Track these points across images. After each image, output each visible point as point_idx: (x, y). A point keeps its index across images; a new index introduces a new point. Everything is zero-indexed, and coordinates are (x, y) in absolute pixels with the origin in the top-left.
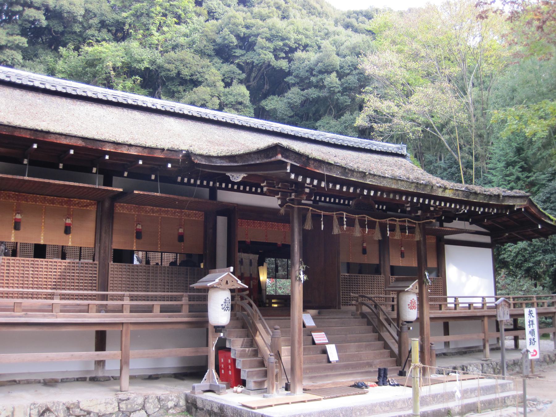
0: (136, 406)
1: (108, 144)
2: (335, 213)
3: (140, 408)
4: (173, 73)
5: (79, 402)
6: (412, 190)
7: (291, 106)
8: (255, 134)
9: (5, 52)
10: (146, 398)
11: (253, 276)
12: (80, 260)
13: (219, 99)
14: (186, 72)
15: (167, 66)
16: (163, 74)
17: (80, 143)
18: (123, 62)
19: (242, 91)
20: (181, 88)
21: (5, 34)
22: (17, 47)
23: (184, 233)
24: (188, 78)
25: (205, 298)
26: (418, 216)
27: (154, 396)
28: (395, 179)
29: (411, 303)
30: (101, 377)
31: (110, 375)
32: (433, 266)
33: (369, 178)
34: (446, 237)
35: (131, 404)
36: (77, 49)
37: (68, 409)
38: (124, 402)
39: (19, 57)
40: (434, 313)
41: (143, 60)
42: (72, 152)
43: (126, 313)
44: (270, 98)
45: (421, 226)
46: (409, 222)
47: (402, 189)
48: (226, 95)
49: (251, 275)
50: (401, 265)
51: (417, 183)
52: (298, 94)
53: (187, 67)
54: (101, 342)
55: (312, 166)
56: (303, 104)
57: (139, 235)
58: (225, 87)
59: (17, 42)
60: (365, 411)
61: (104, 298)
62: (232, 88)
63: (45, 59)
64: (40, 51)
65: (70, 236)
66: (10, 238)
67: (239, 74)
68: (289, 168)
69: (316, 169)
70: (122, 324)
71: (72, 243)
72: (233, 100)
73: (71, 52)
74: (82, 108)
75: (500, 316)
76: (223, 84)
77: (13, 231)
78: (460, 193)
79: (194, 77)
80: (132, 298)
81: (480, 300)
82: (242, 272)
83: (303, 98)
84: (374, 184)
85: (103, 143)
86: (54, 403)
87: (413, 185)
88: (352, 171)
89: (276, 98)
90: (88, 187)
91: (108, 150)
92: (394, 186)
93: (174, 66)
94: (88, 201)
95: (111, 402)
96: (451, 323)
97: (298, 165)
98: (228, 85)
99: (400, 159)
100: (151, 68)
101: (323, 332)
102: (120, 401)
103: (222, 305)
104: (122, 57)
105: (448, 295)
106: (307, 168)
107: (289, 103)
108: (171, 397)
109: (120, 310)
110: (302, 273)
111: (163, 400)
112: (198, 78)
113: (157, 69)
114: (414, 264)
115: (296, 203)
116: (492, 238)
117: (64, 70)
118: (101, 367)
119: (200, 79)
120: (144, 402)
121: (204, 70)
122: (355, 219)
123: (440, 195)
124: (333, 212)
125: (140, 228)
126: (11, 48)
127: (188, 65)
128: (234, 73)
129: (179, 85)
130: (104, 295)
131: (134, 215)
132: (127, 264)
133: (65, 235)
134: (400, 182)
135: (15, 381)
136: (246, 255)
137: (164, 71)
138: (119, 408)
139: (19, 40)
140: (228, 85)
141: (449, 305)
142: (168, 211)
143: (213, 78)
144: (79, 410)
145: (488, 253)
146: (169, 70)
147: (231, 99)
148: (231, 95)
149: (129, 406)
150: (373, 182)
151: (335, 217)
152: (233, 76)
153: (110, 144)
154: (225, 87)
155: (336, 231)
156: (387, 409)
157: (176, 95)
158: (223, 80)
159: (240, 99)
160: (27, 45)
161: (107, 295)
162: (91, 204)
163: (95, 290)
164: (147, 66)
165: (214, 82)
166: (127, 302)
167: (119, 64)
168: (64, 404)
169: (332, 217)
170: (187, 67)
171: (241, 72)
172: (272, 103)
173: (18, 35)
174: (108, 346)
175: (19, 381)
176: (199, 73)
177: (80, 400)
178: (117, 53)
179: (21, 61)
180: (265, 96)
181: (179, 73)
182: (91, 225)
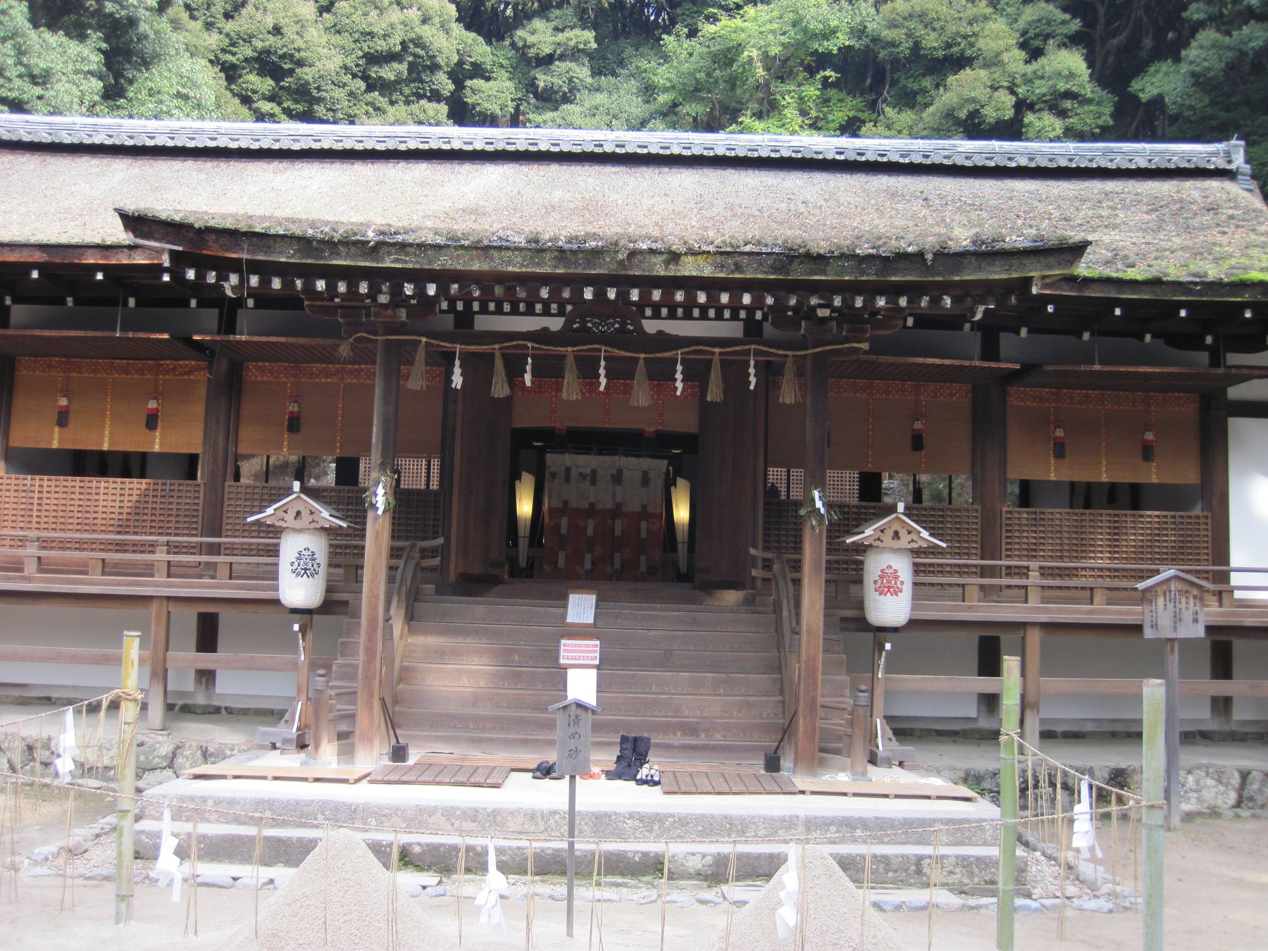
0: (157, 760)
1: (90, 251)
2: (497, 346)
3: (165, 764)
4: (905, 48)
5: (49, 739)
6: (547, 269)
7: (1199, 80)
8: (750, 172)
9: (553, 68)
10: (178, 747)
11: (650, 509)
12: (267, 481)
13: (1013, 93)
14: (931, 41)
15: (888, 34)
16: (882, 54)
17: (39, 257)
18: (783, 44)
19: (1070, 63)
20: (927, 83)
21: (550, 31)
22: (574, 54)
23: (299, 413)
24: (941, 54)
25: (274, 551)
26: (803, 336)
27: (194, 744)
28: (476, 248)
29: (881, 577)
30: (200, 706)
31: (224, 705)
32: (1189, 482)
33: (389, 254)
34: (1236, 392)
35: (145, 753)
36: (693, 33)
37: (30, 748)
39: (582, 72)
40: (1060, 611)
41: (834, 32)
42: (35, 275)
43: (160, 578)
44: (1152, 69)
45: (809, 365)
46: (757, 353)
47: (510, 269)
48: (1031, 81)
49: (644, 507)
50: (1053, 477)
51: (561, 250)
52: (1214, 46)
53: (934, 30)
54: (208, 637)
55: (216, 246)
56: (1232, 67)
57: (294, 424)
58: (1027, 62)
59: (572, 43)
60: (395, 819)
61: (214, 549)
62: (1043, 61)
63: (638, 67)
64: (629, 51)
66: (52, 439)
67: (1063, 22)
69: (227, 250)
70: (151, 598)
71: (161, 446)
72: (1044, 90)
73: (686, 44)
74: (279, 178)
75: (1154, 626)
76: (1021, 55)
77: (57, 429)
78: (745, 260)
79: (955, 49)
80: (173, 548)
82: (619, 499)
83: (1230, 54)
84: (411, 266)
85: (81, 251)
86: (6, 734)
87: (548, 256)
88: (331, 245)
89: (1165, 66)
90: (102, 338)
92: (476, 266)
93: (904, 31)
96: (1240, 647)
98: (1035, 54)
99: (1213, 184)
100: (857, 46)
101: (598, 639)
103: (292, 564)
104: (784, 34)
105: (1235, 561)
106: (205, 252)
107: (1194, 74)
108: (232, 750)
109: (148, 570)
110: (380, 491)
111: (211, 755)
112: (963, 51)
113: (871, 45)
114: (1189, 475)
115: (381, 331)
117: (668, 84)
118: (204, 687)
119: (968, 53)
120: (174, 754)
121: (976, 28)
122: (563, 357)
123: (661, 272)
124: (493, 343)
125: (296, 409)
126: (562, 58)
127: (937, 25)
128: (1049, 23)
129: (924, 75)
130: (211, 545)
131: (286, 383)
132: (119, 480)
134: (496, 254)
135: (49, 699)
136: (632, 460)
137: (883, 48)
139: (576, 36)
140: (1035, 54)
141: (1238, 594)
142: (361, 370)
143: (993, 45)
144: (48, 753)
146: (893, 44)
147: (1041, 88)
148: (1042, 78)
149: (142, 758)
150: (406, 262)
151: (498, 354)
152: (1048, 30)
153: (93, 250)
154: (1027, 62)
155: (500, 389)
156: (467, 825)
157: (919, 99)
158: (1023, 46)
159: (1062, 86)
160: (594, 46)
161: (219, 544)
162: (199, 369)
163: (195, 535)
164: (847, 43)
165: (998, 55)
166: (161, 556)
167: (775, 50)
168: (23, 739)
169: (492, 355)
170: (934, 30)
171: (1067, 17)
172: (1160, 82)
173: (572, 28)
175: (57, 699)
176: (965, 37)
178: (768, 27)
179: (589, 80)
180: (1140, 68)
181: (917, 46)
182: (199, 409)
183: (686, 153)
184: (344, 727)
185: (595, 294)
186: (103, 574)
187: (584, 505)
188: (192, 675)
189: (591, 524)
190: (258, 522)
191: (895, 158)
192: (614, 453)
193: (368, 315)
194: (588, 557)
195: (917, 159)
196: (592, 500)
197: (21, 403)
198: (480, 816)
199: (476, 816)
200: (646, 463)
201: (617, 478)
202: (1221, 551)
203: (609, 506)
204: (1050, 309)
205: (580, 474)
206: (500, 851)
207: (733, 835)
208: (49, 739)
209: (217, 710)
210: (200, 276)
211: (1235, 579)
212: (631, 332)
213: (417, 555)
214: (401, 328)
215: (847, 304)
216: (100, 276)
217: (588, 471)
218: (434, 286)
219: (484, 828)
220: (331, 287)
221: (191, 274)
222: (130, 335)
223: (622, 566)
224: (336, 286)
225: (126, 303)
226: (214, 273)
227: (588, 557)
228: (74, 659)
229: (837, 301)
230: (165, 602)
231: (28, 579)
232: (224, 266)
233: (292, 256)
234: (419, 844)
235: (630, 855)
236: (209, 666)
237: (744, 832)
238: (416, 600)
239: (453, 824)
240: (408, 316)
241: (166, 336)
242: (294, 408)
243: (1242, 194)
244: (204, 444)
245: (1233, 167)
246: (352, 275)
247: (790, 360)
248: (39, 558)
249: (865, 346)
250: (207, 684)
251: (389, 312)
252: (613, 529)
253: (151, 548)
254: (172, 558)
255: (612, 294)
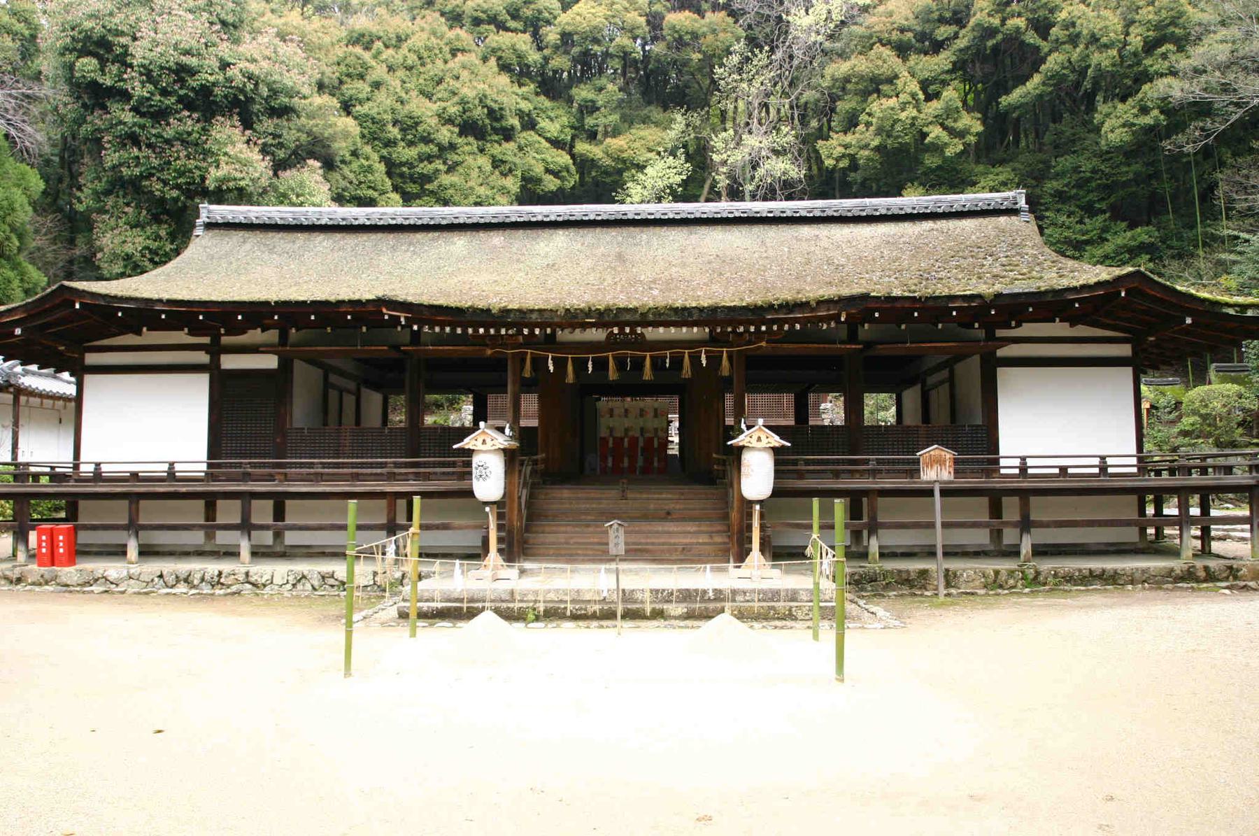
68: (402, 319)
81: (1017, 462)
105: (1002, 453)
116: (1133, 349)
145: (1129, 370)
183: (678, 217)
191: (804, 213)
195: (818, 214)
202: (994, 448)
204: (877, 315)
211: (1003, 462)
215: (747, 331)
243: (1024, 225)
245: (1017, 206)
249: (764, 344)
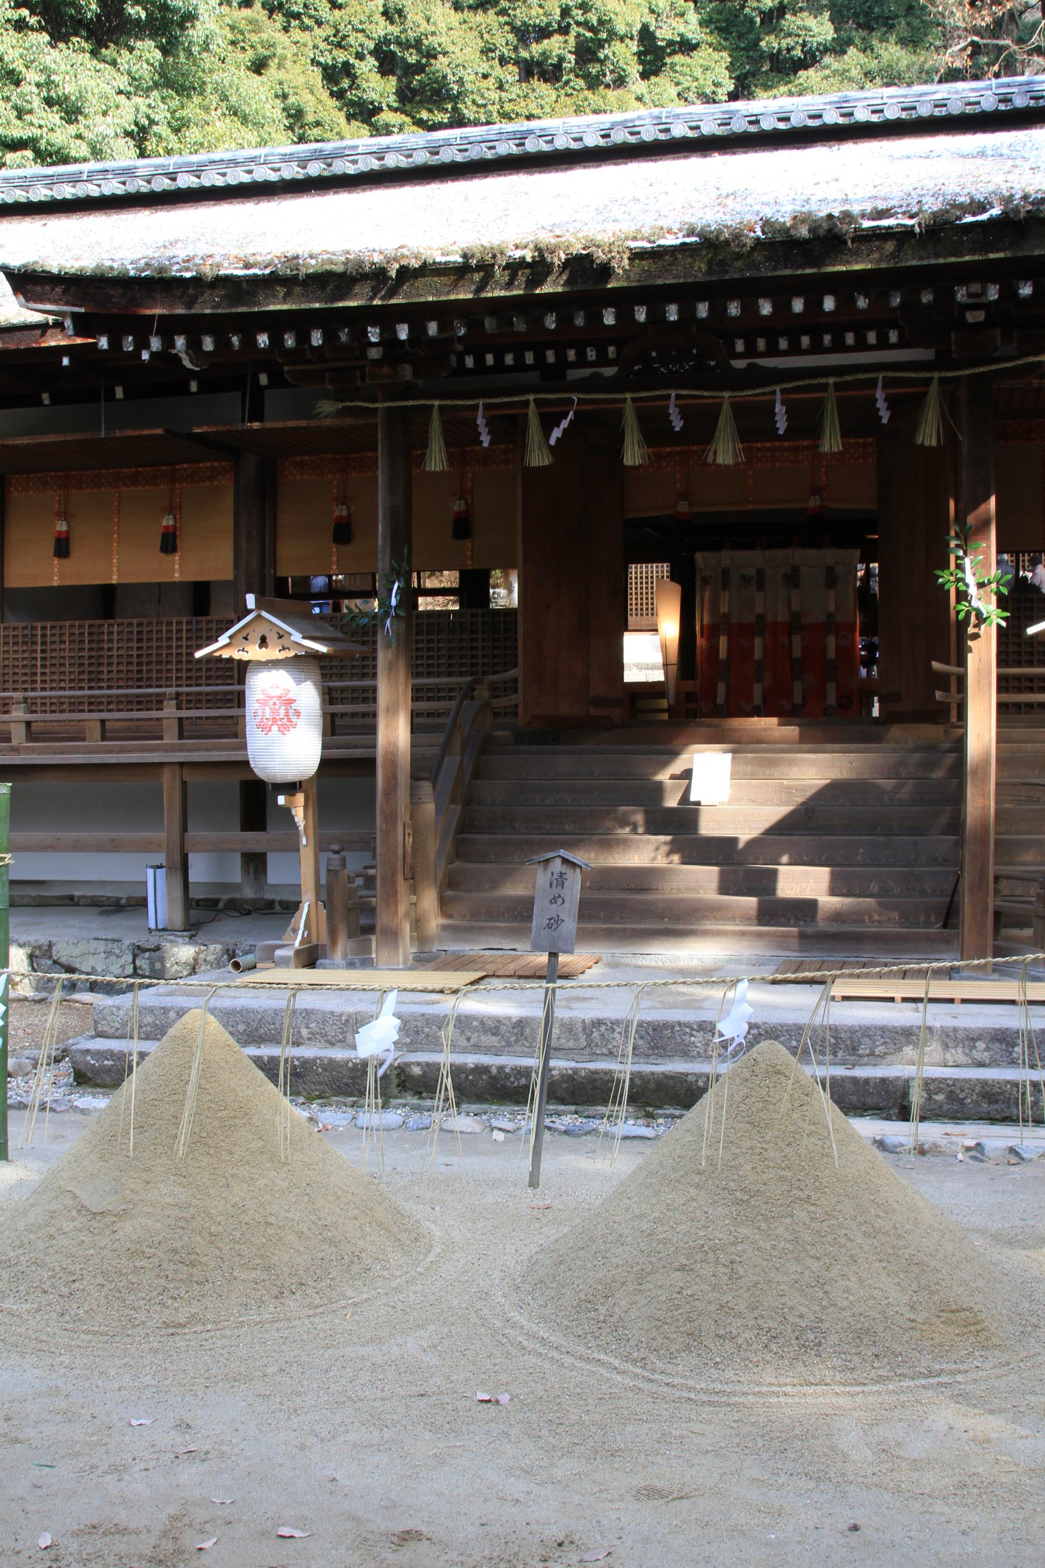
0: (175, 967)
5: (50, 945)
31: (278, 898)
38: (147, 955)
65: (177, 558)
70: (161, 765)
91: (53, 344)
94: (216, 464)
95: (117, 951)
97: (83, 310)
102: (136, 952)
118: (252, 875)
133: (163, 555)
135: (71, 898)
136: (810, 552)
138: (135, 968)
166: (170, 712)
174: (268, 826)
177: (54, 940)
182: (227, 523)
184: (364, 921)
185: (618, 317)
186: (104, 738)
187: (752, 619)
188: (237, 860)
189: (758, 643)
190: (209, 659)
192: (787, 545)
193: (363, 378)
194: (757, 688)
196: (759, 610)
197: (16, 533)
198: (503, 1028)
199: (497, 1028)
200: (830, 556)
201: (793, 579)
203: (783, 617)
205: (743, 577)
206: (457, 1071)
207: (840, 1054)
208: (50, 945)
209: (270, 904)
210: (115, 343)
212: (714, 368)
213: (486, 694)
214: (407, 391)
216: (66, 361)
217: (752, 572)
218: (406, 326)
219: (509, 1044)
220: (276, 340)
221: (104, 343)
222: (118, 434)
223: (804, 699)
224: (282, 340)
225: (111, 396)
226: (130, 338)
227: (757, 688)
228: (77, 847)
229: (993, 293)
230: (177, 769)
231: (16, 750)
232: (142, 329)
233: (218, 305)
234: (419, 1064)
235: (690, 1078)
236: (258, 849)
237: (854, 1049)
238: (484, 751)
239: (468, 1039)
240: (416, 373)
241: (159, 431)
242: (341, 511)
244: (236, 567)
246: (301, 322)
247: (934, 390)
248: (28, 724)
250: (256, 872)
251: (386, 370)
252: (790, 650)
253: (158, 702)
254: (184, 713)
255: (672, 313)
